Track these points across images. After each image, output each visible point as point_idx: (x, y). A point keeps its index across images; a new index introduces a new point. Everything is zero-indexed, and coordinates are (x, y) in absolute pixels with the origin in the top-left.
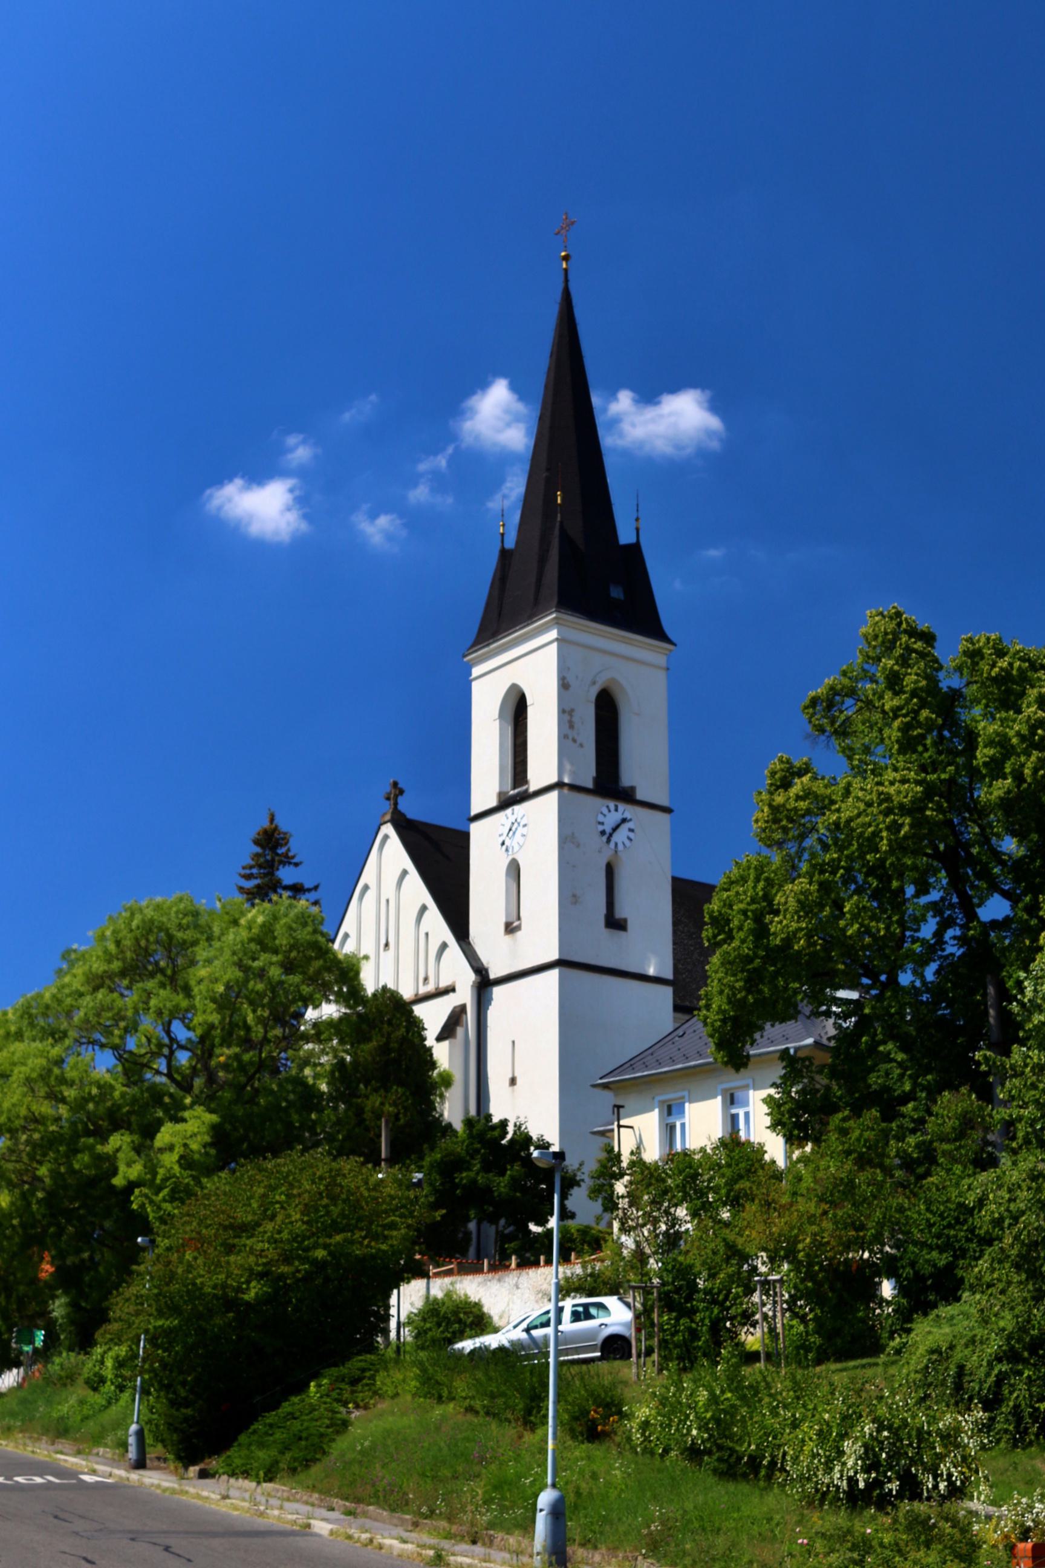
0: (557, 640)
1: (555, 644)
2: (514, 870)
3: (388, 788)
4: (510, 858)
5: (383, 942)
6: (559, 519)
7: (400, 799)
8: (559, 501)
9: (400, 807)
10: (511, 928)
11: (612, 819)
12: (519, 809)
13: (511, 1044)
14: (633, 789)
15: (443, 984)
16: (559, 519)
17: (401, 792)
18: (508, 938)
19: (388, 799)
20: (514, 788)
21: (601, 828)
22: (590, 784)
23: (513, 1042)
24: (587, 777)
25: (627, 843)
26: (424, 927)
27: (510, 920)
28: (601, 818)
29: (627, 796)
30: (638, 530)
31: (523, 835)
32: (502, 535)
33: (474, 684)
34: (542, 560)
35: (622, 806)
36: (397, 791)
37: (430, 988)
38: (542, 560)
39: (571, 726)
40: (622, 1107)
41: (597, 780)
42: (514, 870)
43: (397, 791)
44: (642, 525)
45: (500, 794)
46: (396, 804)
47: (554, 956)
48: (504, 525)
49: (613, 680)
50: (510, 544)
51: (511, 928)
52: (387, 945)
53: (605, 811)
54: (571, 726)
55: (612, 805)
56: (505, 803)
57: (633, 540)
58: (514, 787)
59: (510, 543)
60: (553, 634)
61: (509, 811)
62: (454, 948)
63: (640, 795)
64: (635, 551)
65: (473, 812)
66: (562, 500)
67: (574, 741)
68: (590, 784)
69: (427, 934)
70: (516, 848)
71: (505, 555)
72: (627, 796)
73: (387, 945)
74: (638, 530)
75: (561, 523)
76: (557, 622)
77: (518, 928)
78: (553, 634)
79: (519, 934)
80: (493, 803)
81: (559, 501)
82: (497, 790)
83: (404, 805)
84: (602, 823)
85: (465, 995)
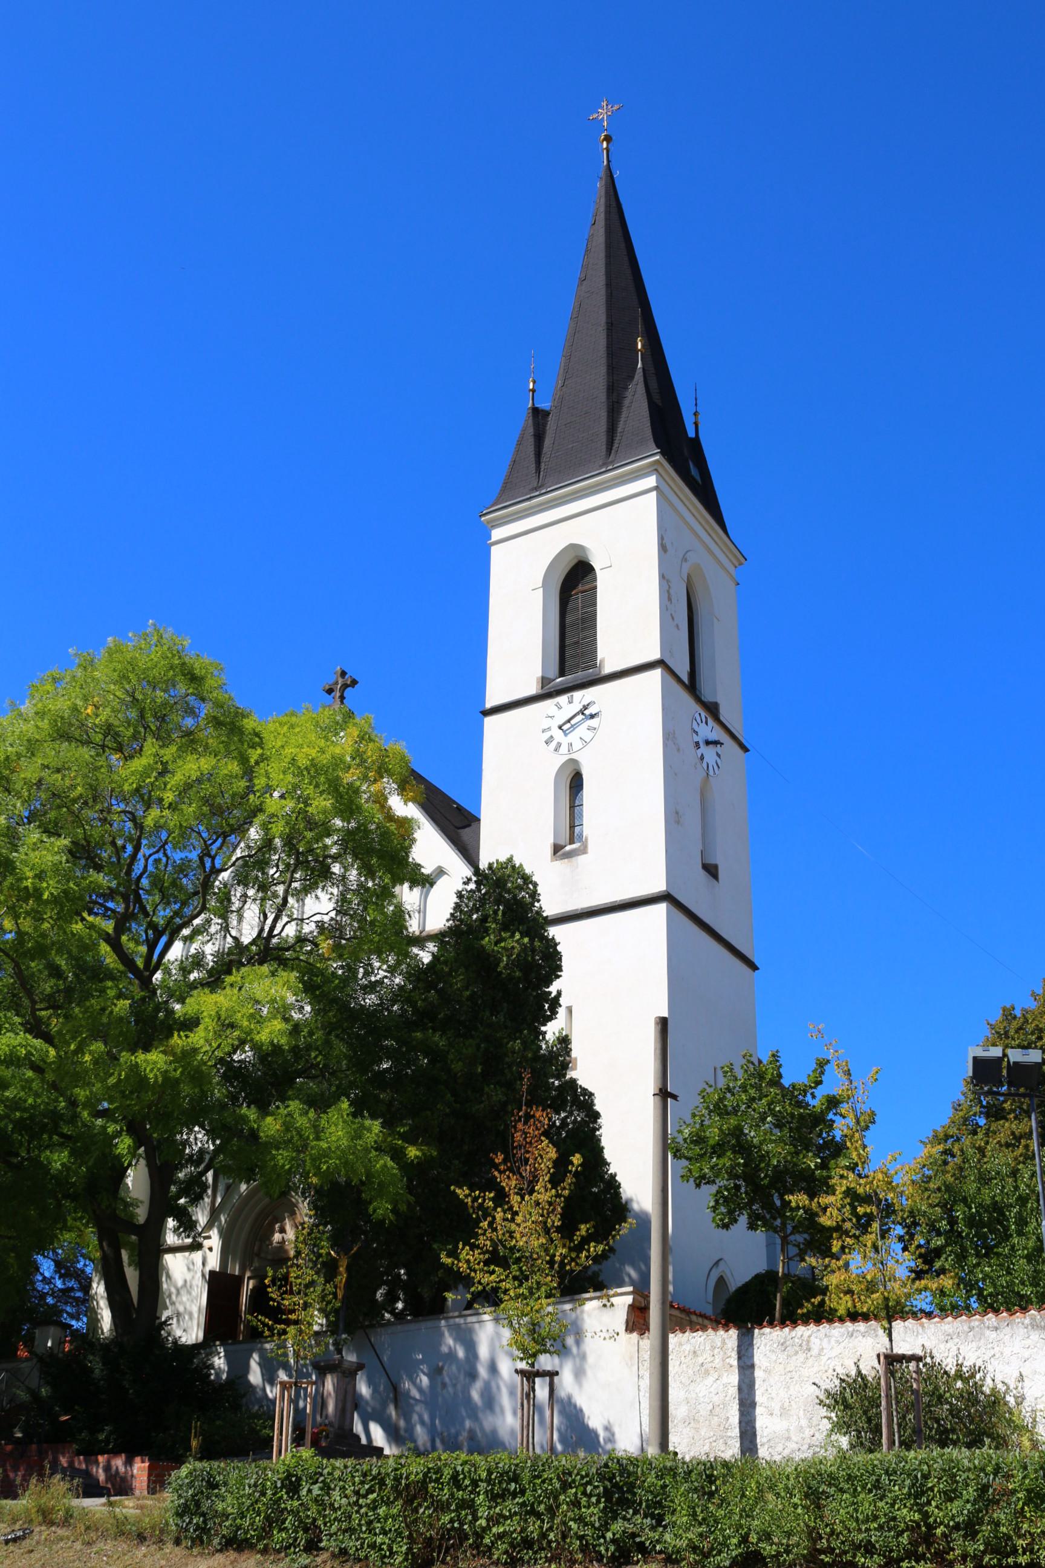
0: (656, 488)
1: (654, 493)
6: (640, 365)
8: (639, 347)
12: (581, 697)
16: (640, 365)
17: (354, 683)
18: (560, 865)
19: (330, 691)
20: (562, 674)
21: (696, 739)
24: (683, 670)
25: (716, 767)
27: (562, 843)
32: (533, 391)
33: (493, 549)
34: (614, 410)
38: (614, 410)
39: (670, 599)
44: (700, 418)
45: (544, 681)
46: (342, 698)
47: (659, 885)
48: (534, 382)
54: (670, 599)
55: (703, 714)
56: (548, 692)
58: (562, 674)
59: (544, 405)
60: (651, 481)
61: (563, 699)
63: (725, 714)
64: (696, 444)
65: (489, 705)
66: (643, 346)
67: (673, 619)
70: (577, 745)
72: (712, 710)
75: (644, 369)
76: (654, 469)
78: (651, 481)
79: (581, 859)
80: (533, 689)
81: (639, 347)
82: (540, 674)
84: (696, 733)
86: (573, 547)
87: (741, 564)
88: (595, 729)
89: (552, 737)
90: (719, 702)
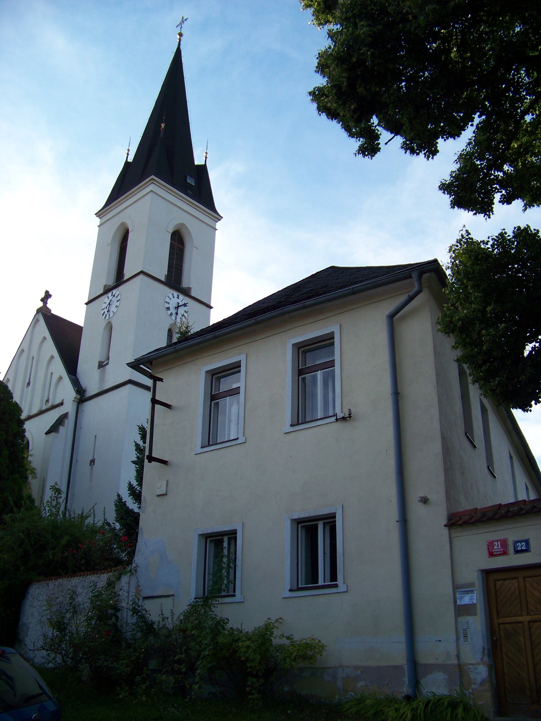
2: (110, 327)
3: (43, 295)
4: (107, 321)
5: (27, 381)
7: (49, 301)
9: (48, 305)
10: (101, 365)
11: (173, 303)
13: (94, 437)
14: (189, 289)
15: (58, 401)
21: (167, 306)
22: (163, 279)
23: (96, 436)
24: (162, 273)
26: (52, 369)
28: (168, 300)
29: (186, 292)
30: (206, 157)
31: (117, 307)
35: (181, 297)
36: (48, 295)
37: (50, 404)
40: (161, 380)
41: (168, 276)
42: (110, 327)
43: (48, 295)
45: (105, 286)
49: (183, 225)
50: (131, 159)
51: (101, 365)
52: (29, 384)
53: (171, 296)
55: (176, 294)
56: (107, 290)
57: (203, 163)
61: (110, 294)
62: (67, 381)
63: (193, 294)
68: (163, 279)
69: (52, 373)
71: (127, 164)
72: (186, 292)
73: (29, 384)
74: (206, 157)
77: (107, 364)
79: (107, 366)
83: (51, 304)
84: (169, 303)
85: (69, 407)
86: (123, 224)
87: (219, 220)
88: (117, 306)
89: (104, 312)
90: (191, 286)
